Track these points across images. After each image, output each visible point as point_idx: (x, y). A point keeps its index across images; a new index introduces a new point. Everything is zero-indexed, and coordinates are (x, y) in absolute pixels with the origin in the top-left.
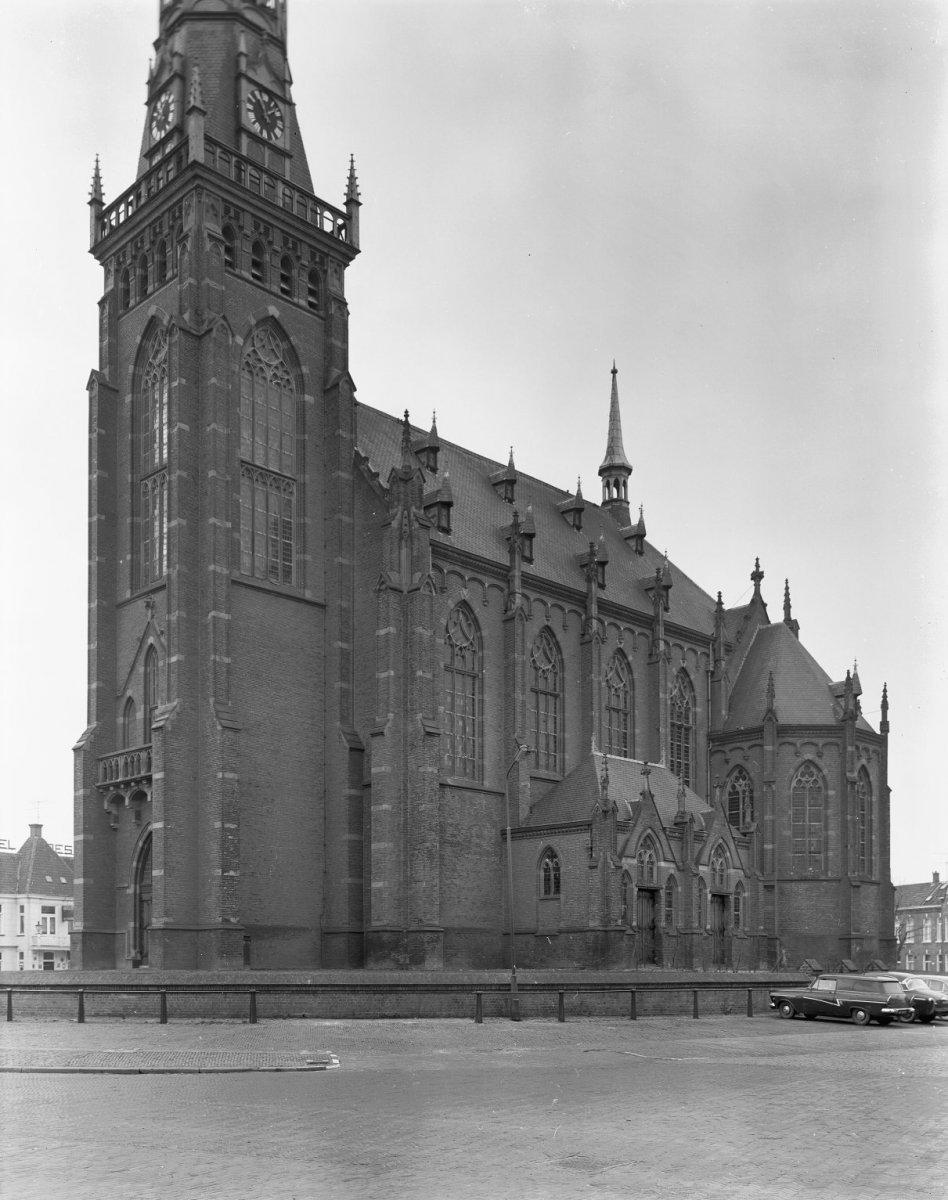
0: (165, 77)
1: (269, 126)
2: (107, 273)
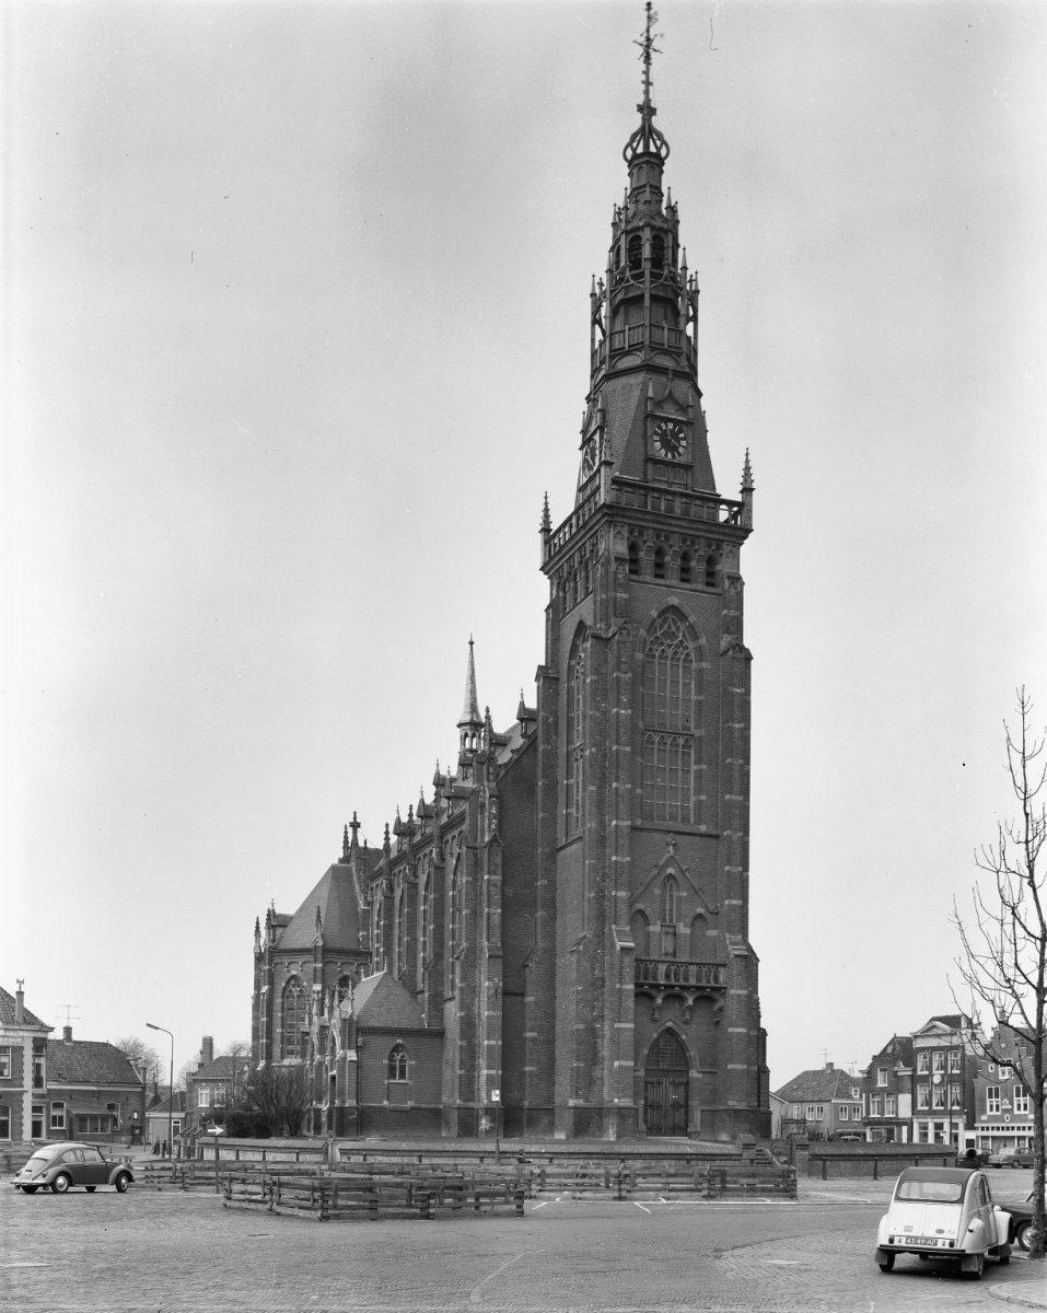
2: (552, 584)
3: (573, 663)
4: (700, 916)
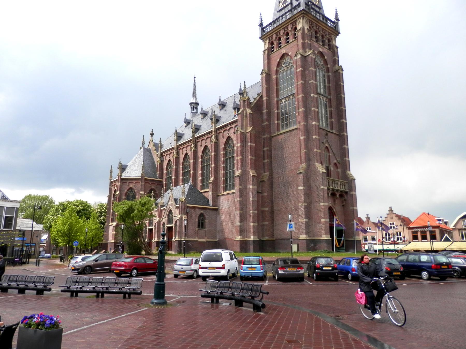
3: (278, 69)
4: (335, 164)
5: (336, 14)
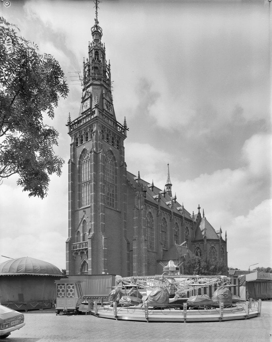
0: (87, 97)
1: (109, 110)
2: (72, 138)
3: (81, 160)
5: (125, 121)
